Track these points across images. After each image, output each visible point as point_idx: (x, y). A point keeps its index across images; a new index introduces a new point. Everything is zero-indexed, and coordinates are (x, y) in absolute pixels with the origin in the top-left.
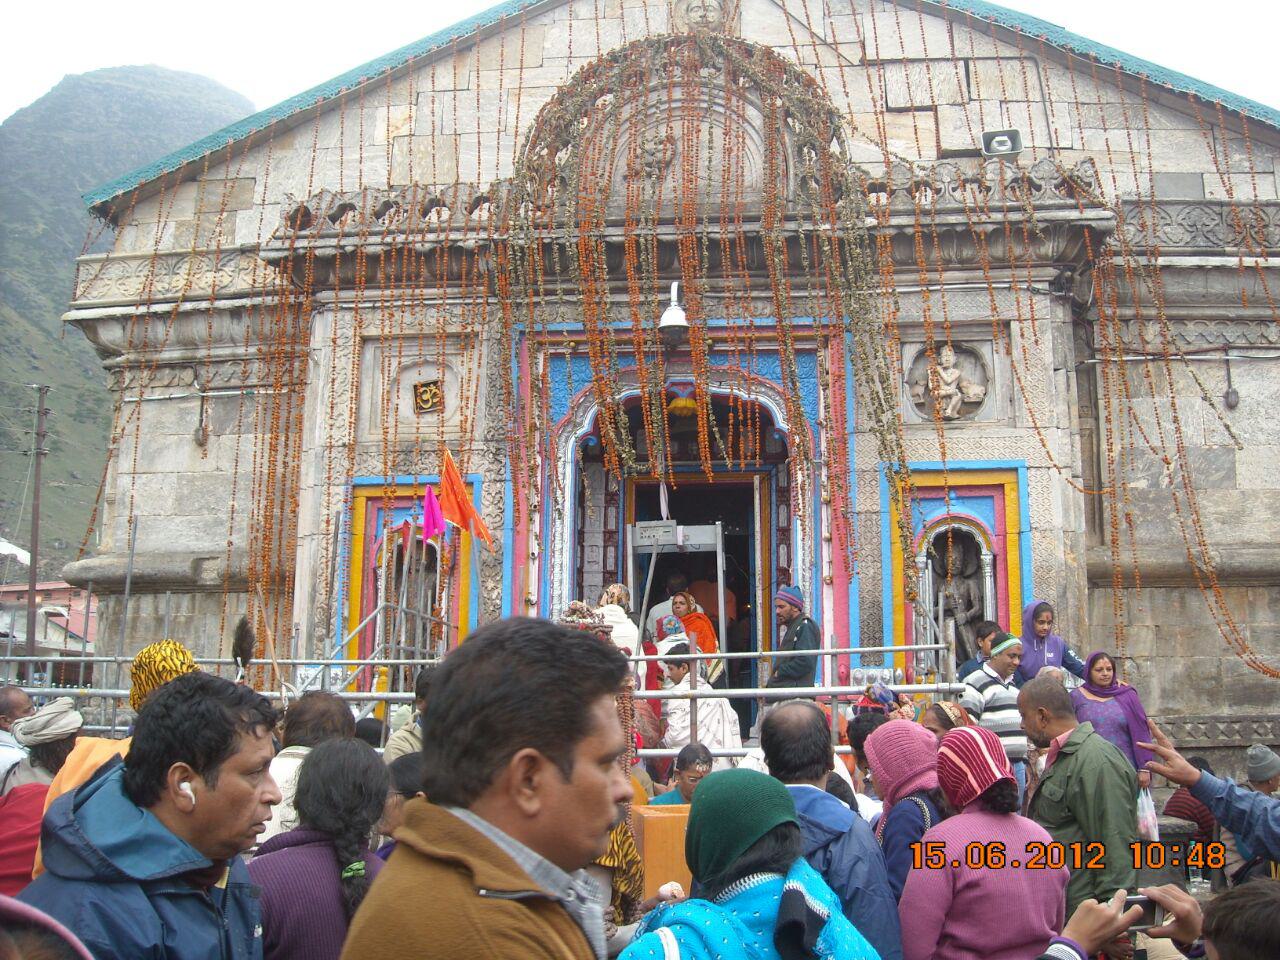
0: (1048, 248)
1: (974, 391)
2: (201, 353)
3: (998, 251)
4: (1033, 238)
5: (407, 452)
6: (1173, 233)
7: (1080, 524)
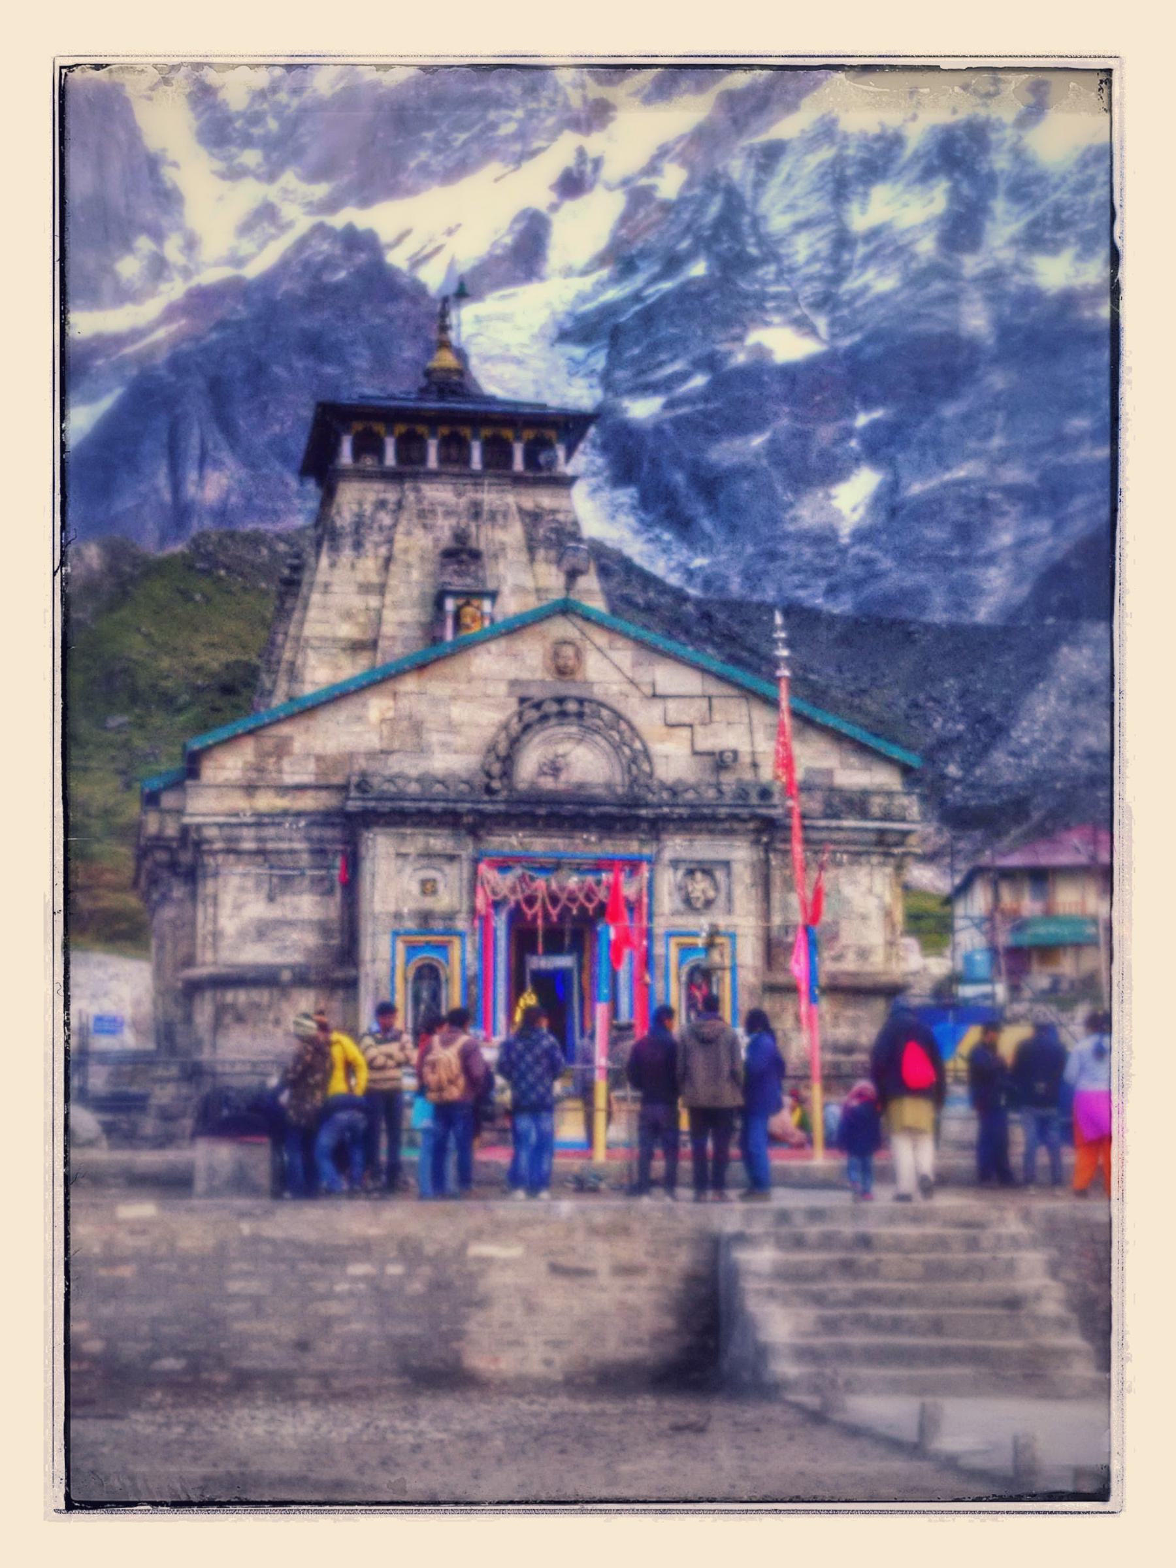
0: (751, 825)
1: (711, 894)
2: (270, 846)
3: (727, 825)
4: (744, 821)
5: (425, 917)
6: (814, 805)
7: (759, 963)
